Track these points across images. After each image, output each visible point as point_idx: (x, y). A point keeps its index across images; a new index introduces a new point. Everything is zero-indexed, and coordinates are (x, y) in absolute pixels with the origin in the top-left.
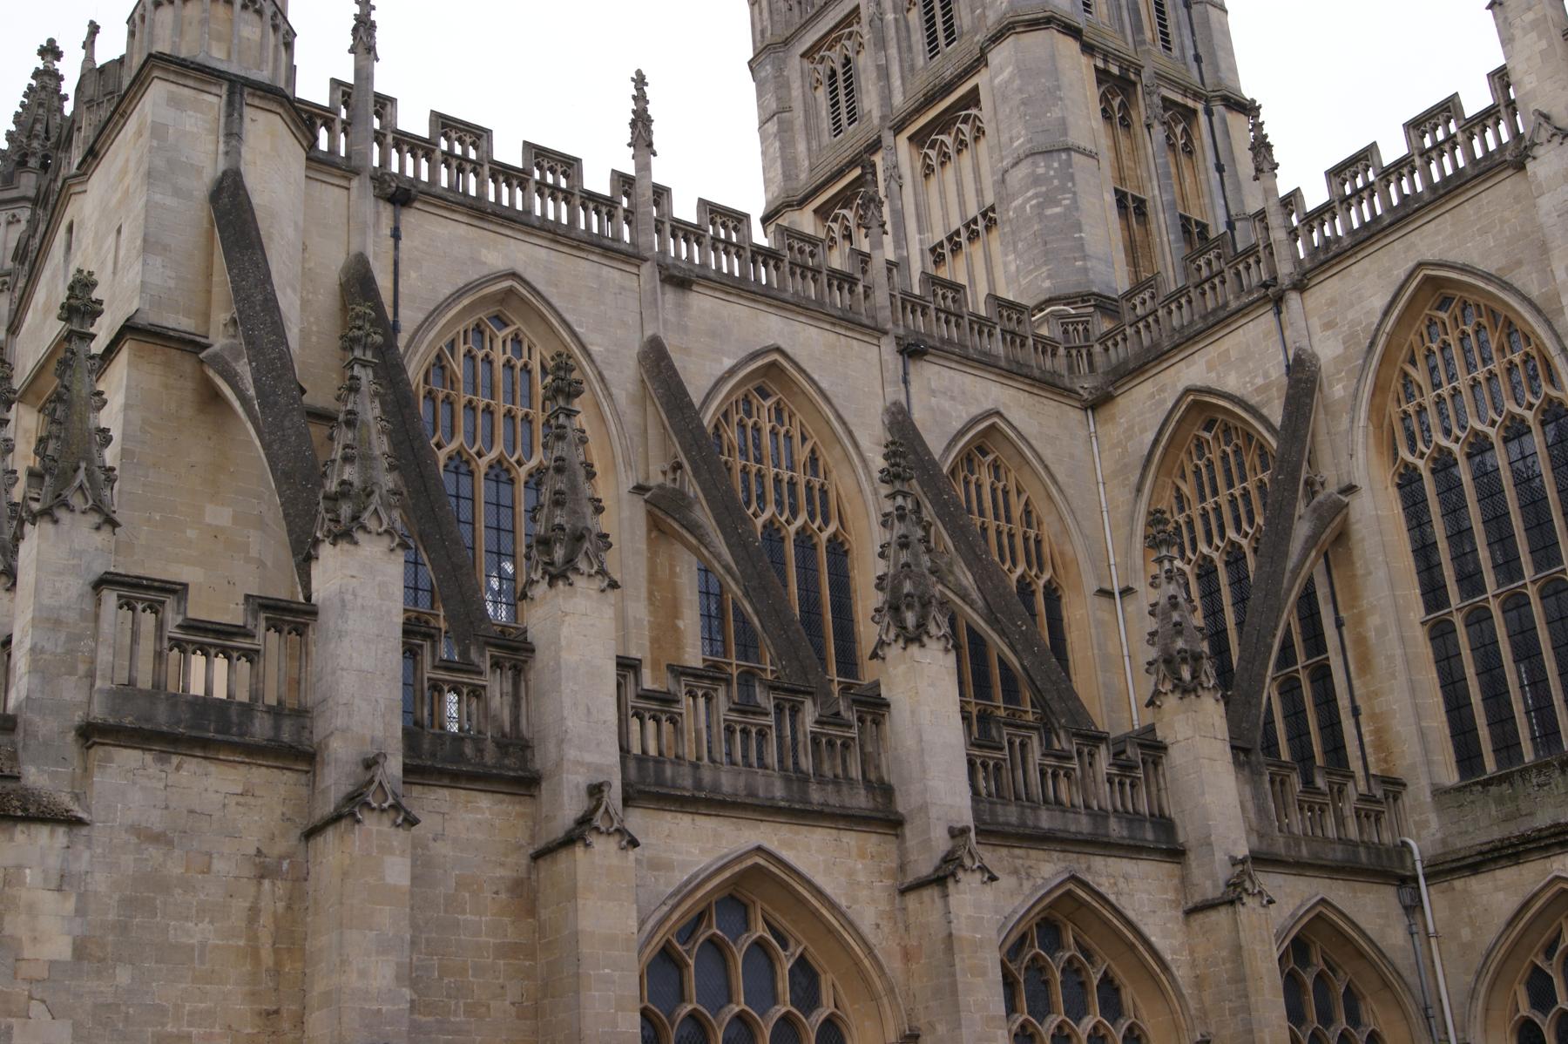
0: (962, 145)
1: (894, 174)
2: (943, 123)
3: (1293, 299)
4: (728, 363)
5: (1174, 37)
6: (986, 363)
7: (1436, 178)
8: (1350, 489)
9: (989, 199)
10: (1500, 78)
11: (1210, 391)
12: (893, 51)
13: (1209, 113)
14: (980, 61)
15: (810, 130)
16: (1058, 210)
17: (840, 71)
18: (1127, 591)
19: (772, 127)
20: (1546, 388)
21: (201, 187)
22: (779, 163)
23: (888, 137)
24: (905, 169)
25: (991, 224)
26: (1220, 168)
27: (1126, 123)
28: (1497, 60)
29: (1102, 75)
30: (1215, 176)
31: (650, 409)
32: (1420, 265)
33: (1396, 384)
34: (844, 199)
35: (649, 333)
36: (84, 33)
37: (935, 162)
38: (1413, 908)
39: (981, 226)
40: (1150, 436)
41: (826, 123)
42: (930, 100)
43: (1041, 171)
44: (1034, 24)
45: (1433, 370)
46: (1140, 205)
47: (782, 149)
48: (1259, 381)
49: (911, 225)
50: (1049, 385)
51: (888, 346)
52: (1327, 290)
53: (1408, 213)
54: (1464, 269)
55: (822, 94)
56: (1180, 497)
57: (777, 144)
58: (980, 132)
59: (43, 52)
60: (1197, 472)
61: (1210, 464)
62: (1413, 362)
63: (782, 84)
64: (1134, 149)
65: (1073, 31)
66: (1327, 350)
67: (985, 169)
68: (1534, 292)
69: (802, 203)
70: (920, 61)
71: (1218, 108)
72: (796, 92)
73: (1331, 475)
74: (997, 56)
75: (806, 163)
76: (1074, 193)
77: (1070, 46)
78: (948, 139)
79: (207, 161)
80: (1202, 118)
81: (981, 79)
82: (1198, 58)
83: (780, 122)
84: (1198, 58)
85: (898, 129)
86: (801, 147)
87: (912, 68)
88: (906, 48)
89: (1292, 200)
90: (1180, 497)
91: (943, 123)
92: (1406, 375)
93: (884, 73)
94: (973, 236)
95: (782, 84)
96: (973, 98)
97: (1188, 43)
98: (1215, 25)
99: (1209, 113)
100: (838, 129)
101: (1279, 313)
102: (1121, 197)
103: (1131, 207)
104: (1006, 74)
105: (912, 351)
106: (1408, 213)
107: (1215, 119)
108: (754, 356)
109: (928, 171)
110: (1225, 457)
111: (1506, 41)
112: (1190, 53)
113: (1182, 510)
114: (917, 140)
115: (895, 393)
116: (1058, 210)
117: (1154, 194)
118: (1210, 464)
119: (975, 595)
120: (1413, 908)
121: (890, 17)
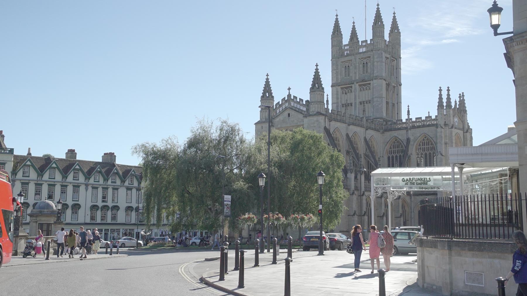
0: (367, 89)
1: (355, 89)
2: (364, 85)
3: (409, 131)
4: (352, 134)
5: (394, 74)
6: (372, 129)
7: (427, 124)
8: (412, 154)
9: (370, 99)
10: (436, 116)
11: (397, 137)
12: (357, 70)
13: (397, 86)
16: (380, 106)
18: (383, 157)
19: (335, 72)
20: (434, 150)
21: (323, 128)
22: (335, 78)
23: (355, 83)
24: (357, 89)
25: (370, 103)
26: (397, 95)
27: (388, 90)
28: (437, 115)
29: (386, 84)
30: (396, 96)
31: (347, 141)
32: (424, 133)
33: (419, 144)
34: (346, 88)
35: (347, 132)
37: (362, 90)
38: (411, 198)
39: (368, 102)
40: (388, 140)
41: (344, 74)
42: (363, 81)
43: (379, 100)
45: (423, 143)
46: (388, 102)
47: (336, 76)
48: (403, 138)
49: (357, 98)
50: (378, 131)
51: (365, 129)
52: (413, 131)
53: (424, 126)
54: (429, 136)
55: (343, 69)
56: (391, 147)
57: (336, 75)
58: (370, 89)
59: (266, 75)
60: (393, 145)
61: (395, 145)
62: (421, 142)
63: (337, 65)
64: (388, 94)
65: (385, 80)
66: (412, 138)
68: (435, 141)
69: (339, 86)
72: (339, 67)
73: (409, 153)
74: (375, 81)
75: (340, 80)
76: (382, 104)
77: (384, 81)
78: (365, 87)
79: (323, 125)
80: (396, 87)
81: (371, 82)
82: (397, 77)
83: (336, 71)
84: (397, 77)
85: (357, 83)
86: (339, 77)
87: (360, 74)
89: (411, 119)
90: (391, 147)
91: (364, 85)
92: (420, 143)
93: (355, 73)
94: (367, 103)
95: (337, 65)
96: (370, 84)
97: (396, 75)
98: (399, 71)
99: (397, 86)
100: (346, 76)
101: (407, 131)
102: (386, 101)
103: (387, 103)
104: (376, 84)
105: (366, 130)
106: (424, 126)
107: (398, 87)
108: (354, 133)
109: (361, 90)
110: (397, 145)
111: (438, 114)
112: (396, 77)
113: (391, 149)
114: (360, 85)
115: (365, 136)
116: (380, 106)
117: (390, 101)
118: (395, 145)
119: (374, 162)
120: (411, 198)
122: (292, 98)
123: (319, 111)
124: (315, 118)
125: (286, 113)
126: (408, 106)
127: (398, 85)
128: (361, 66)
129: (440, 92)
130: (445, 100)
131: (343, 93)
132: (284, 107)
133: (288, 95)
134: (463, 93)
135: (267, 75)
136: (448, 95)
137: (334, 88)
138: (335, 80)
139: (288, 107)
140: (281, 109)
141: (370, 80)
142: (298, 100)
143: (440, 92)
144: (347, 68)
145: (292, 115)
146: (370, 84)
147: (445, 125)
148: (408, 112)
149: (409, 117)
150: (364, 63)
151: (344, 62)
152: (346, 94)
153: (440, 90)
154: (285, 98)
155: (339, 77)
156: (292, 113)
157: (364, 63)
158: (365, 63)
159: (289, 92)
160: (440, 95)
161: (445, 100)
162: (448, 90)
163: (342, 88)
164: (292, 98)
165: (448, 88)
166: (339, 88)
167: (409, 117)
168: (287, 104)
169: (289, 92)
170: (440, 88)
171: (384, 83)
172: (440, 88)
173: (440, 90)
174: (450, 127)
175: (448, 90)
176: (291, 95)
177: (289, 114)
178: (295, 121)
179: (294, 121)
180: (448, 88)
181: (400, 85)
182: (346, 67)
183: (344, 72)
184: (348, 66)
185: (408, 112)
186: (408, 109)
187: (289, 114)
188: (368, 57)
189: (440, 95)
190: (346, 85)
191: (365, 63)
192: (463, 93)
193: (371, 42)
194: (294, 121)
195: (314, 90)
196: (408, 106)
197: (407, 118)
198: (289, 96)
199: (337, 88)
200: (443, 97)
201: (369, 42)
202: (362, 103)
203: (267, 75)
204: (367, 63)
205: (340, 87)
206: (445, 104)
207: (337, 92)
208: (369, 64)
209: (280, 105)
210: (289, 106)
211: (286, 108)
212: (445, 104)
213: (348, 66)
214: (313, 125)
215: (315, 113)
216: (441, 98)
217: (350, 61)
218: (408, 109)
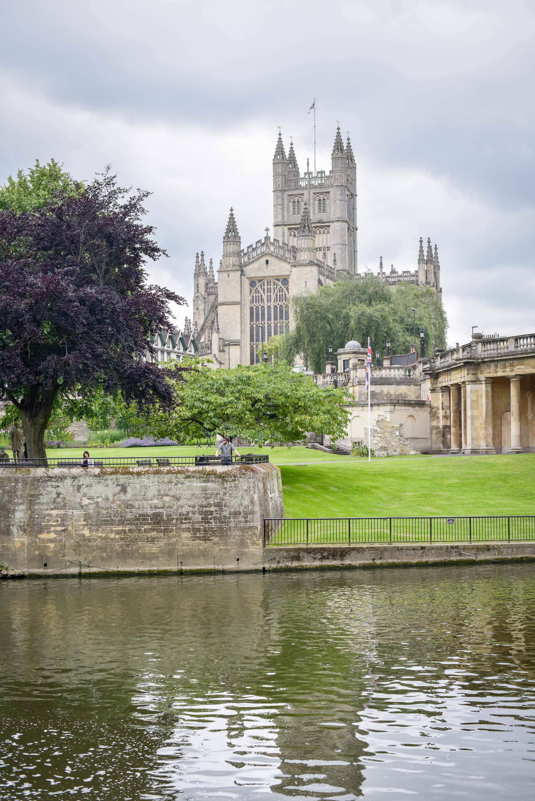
2: (321, 227)
9: (329, 245)
12: (312, 208)
14: (333, 222)
15: (288, 211)
17: (296, 203)
25: (328, 250)
34: (296, 229)
36: (265, 228)
41: (291, 211)
42: (319, 222)
44: (344, 221)
55: (291, 205)
58: (328, 233)
67: (329, 239)
69: (285, 225)
70: (317, 211)
71: (355, 230)
78: (322, 230)
86: (286, 214)
88: (314, 208)
96: (329, 226)
104: (338, 228)
121: (312, 201)
122: (272, 241)
123: (312, 260)
124: (308, 268)
125: (263, 260)
126: (381, 258)
127: (355, 230)
128: (317, 203)
129: (421, 244)
130: (425, 254)
131: (290, 235)
132: (259, 251)
133: (265, 238)
134: (436, 245)
135: (232, 210)
136: (430, 247)
137: (280, 229)
138: (281, 218)
139: (265, 253)
140: (255, 254)
141: (330, 222)
142: (281, 244)
143: (421, 244)
144: (296, 203)
145: (272, 263)
146: (329, 226)
147: (428, 283)
148: (381, 264)
149: (381, 271)
150: (320, 200)
151: (292, 195)
152: (295, 236)
153: (421, 241)
154: (260, 241)
155: (286, 214)
156: (271, 260)
157: (320, 200)
158: (322, 199)
159: (267, 234)
160: (421, 247)
161: (425, 254)
162: (429, 242)
163: (289, 229)
164: (272, 241)
165: (429, 239)
166: (286, 228)
167: (381, 271)
168: (264, 249)
169: (267, 234)
170: (421, 238)
171: (347, 226)
172: (421, 238)
173: (421, 241)
174: (432, 285)
175: (429, 242)
176: (270, 237)
177: (267, 262)
178: (277, 270)
179: (274, 270)
180: (429, 239)
181: (357, 229)
182: (294, 202)
183: (291, 208)
184: (298, 202)
185: (381, 264)
186: (381, 261)
187: (267, 262)
188: (326, 193)
189: (421, 247)
190: (296, 224)
191: (322, 199)
192: (436, 245)
193: (330, 174)
194: (274, 270)
195: (305, 234)
196: (381, 258)
197: (379, 272)
198: (267, 238)
199: (283, 229)
200: (423, 249)
201: (327, 174)
202: (318, 249)
203: (232, 210)
204: (324, 200)
205: (286, 227)
206: (425, 258)
207: (283, 233)
208: (327, 202)
209: (253, 250)
210: (267, 251)
211: (263, 255)
212: (425, 258)
213: (298, 202)
214: (305, 276)
215: (307, 261)
216: (421, 251)
217: (300, 194)
218: (381, 261)
